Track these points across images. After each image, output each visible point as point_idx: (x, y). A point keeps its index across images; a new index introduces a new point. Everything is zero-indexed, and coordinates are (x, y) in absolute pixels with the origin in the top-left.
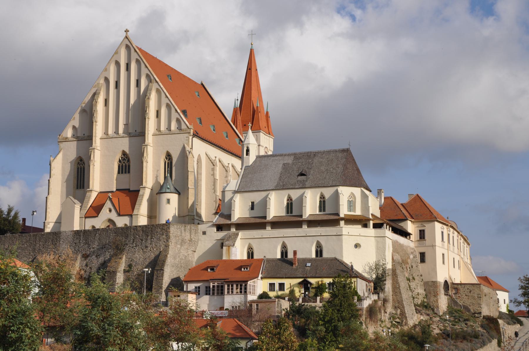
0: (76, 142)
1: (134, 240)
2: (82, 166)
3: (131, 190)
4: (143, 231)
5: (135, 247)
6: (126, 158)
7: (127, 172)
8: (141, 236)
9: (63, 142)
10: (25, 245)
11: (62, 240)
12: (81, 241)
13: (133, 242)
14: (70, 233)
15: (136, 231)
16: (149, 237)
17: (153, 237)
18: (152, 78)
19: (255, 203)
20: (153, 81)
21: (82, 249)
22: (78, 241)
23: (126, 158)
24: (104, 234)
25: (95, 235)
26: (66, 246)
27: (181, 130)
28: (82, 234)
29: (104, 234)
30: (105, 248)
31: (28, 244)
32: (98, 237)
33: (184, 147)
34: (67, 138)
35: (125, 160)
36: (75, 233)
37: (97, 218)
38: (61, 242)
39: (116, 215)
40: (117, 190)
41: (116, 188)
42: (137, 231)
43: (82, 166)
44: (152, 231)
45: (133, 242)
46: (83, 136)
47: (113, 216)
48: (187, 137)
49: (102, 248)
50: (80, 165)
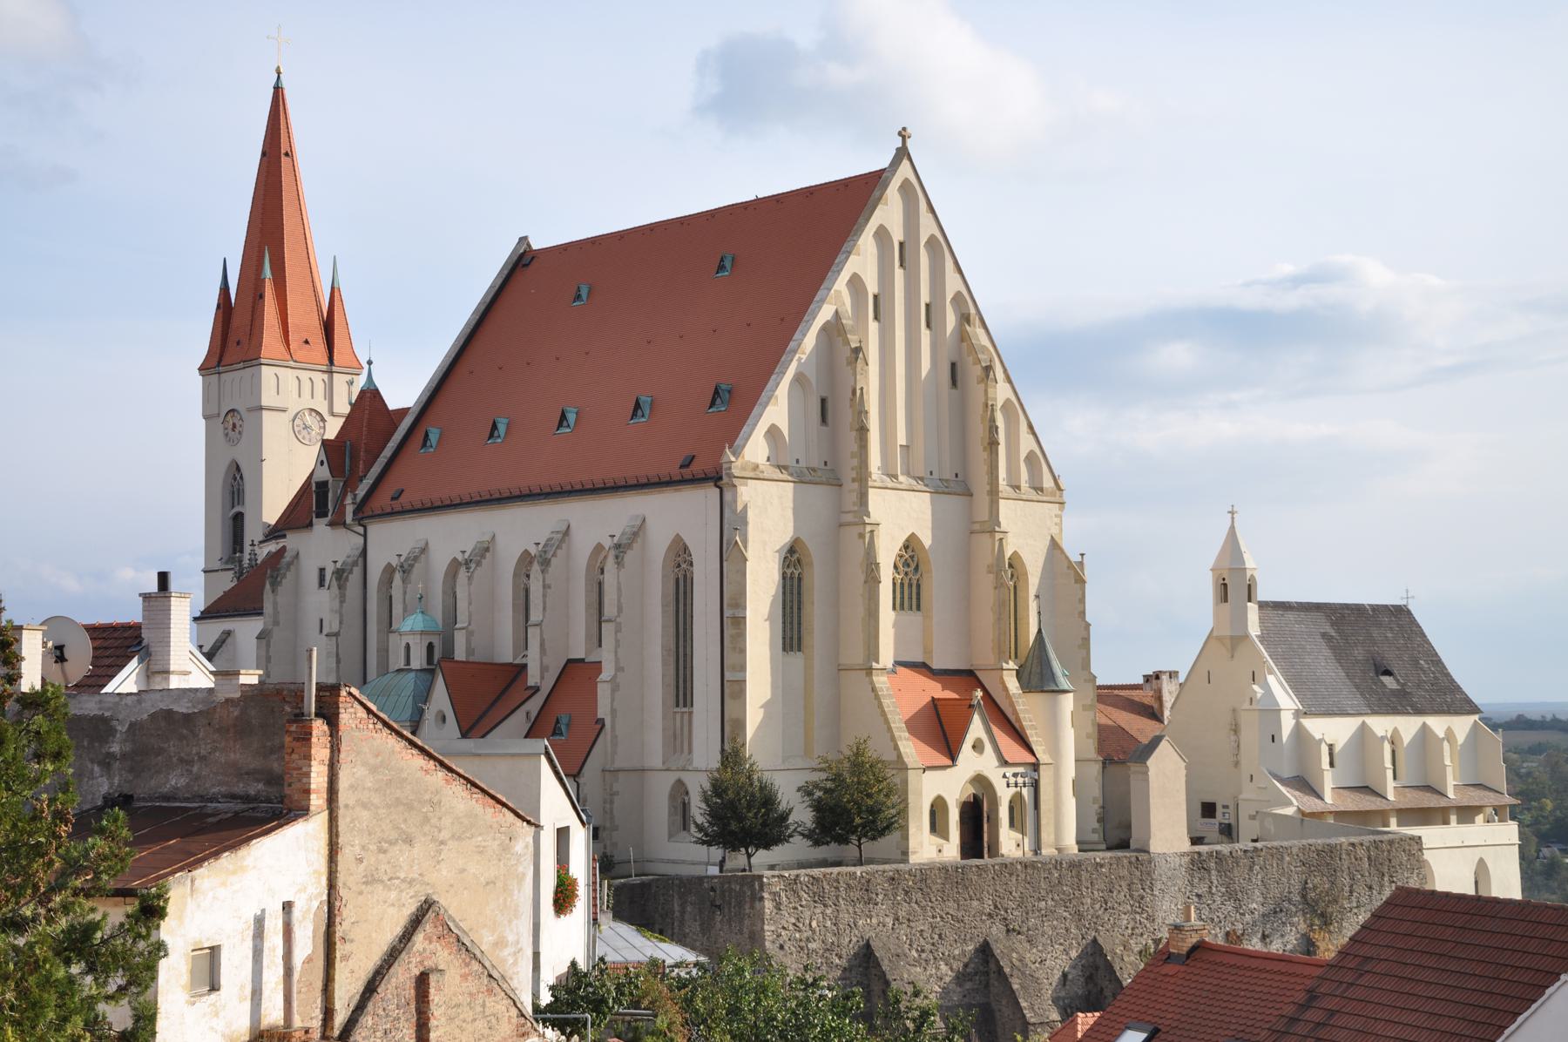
0: (792, 484)
1: (1351, 886)
2: (796, 573)
3: (935, 666)
4: (1369, 858)
5: (1355, 911)
6: (910, 561)
7: (914, 606)
8: (1367, 874)
9: (749, 481)
10: (1050, 902)
11: (1158, 885)
12: (1214, 890)
13: (1351, 892)
14: (1177, 859)
15: (1354, 860)
16: (1386, 879)
17: (1395, 879)
18: (973, 311)
19: (1337, 749)
20: (975, 319)
21: (1220, 914)
22: (1202, 889)
23: (910, 561)
24: (1275, 865)
25: (1251, 869)
26: (1173, 907)
27: (1042, 490)
28: (1213, 865)
29: (1275, 865)
30: (1281, 911)
31: (1056, 897)
32: (1259, 877)
33: (1054, 545)
34: (756, 467)
35: (908, 566)
36: (1192, 861)
37: (953, 769)
38: (1156, 893)
39: (997, 764)
40: (898, 663)
41: (895, 656)
42: (1356, 859)
43: (796, 573)
44: (1390, 860)
45: (1351, 892)
46: (794, 464)
47: (986, 764)
48: (1056, 516)
49: (1275, 912)
50: (788, 567)
